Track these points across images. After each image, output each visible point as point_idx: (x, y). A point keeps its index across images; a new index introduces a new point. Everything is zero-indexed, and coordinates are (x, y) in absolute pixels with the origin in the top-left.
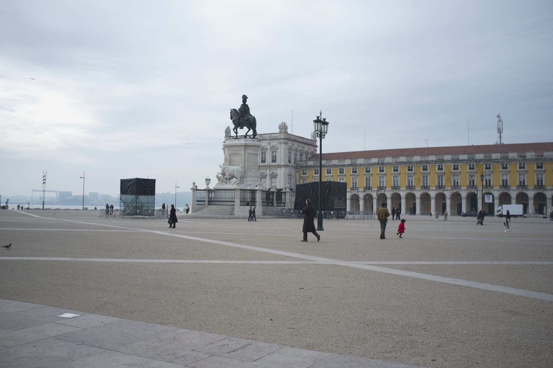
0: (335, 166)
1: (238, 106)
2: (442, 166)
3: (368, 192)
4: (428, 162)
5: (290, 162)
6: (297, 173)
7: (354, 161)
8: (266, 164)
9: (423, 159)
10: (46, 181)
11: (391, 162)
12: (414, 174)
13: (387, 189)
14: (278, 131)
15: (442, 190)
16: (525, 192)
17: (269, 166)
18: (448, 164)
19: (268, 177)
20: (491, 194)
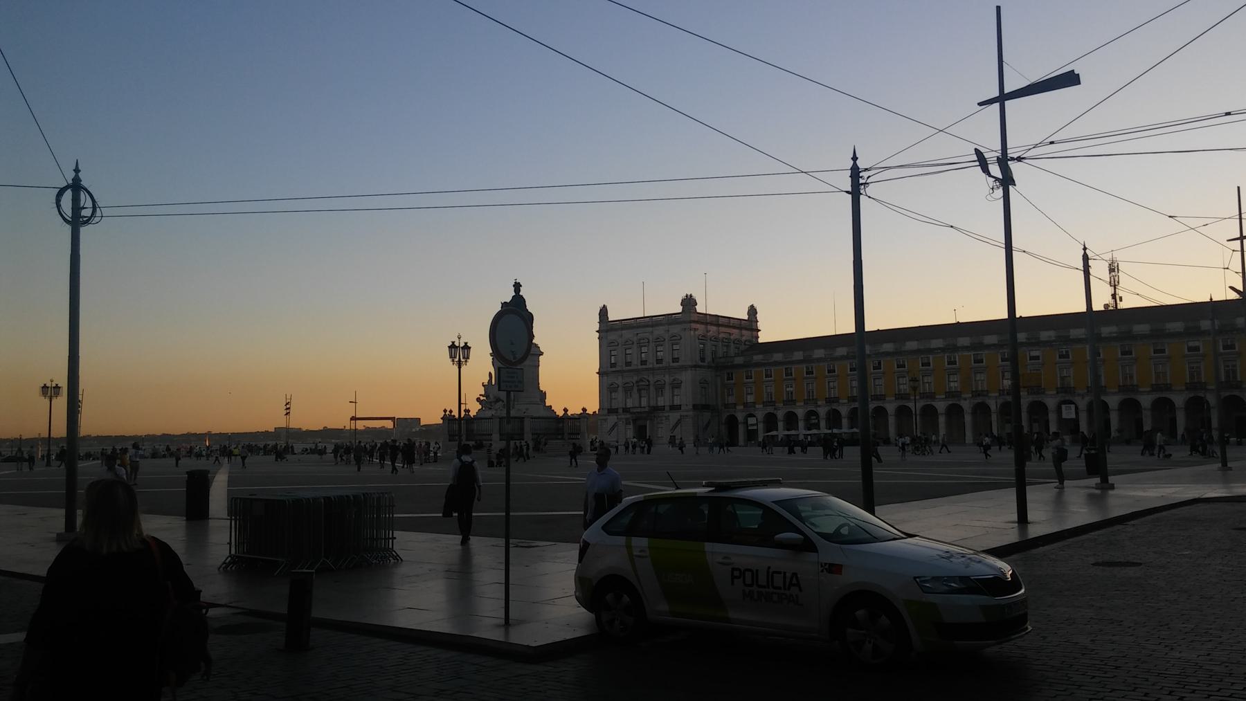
0: (777, 363)
1: (508, 296)
3: (835, 406)
4: (931, 351)
5: (703, 360)
8: (664, 364)
9: (922, 347)
10: (292, 411)
14: (679, 309)
18: (966, 353)
19: (667, 387)
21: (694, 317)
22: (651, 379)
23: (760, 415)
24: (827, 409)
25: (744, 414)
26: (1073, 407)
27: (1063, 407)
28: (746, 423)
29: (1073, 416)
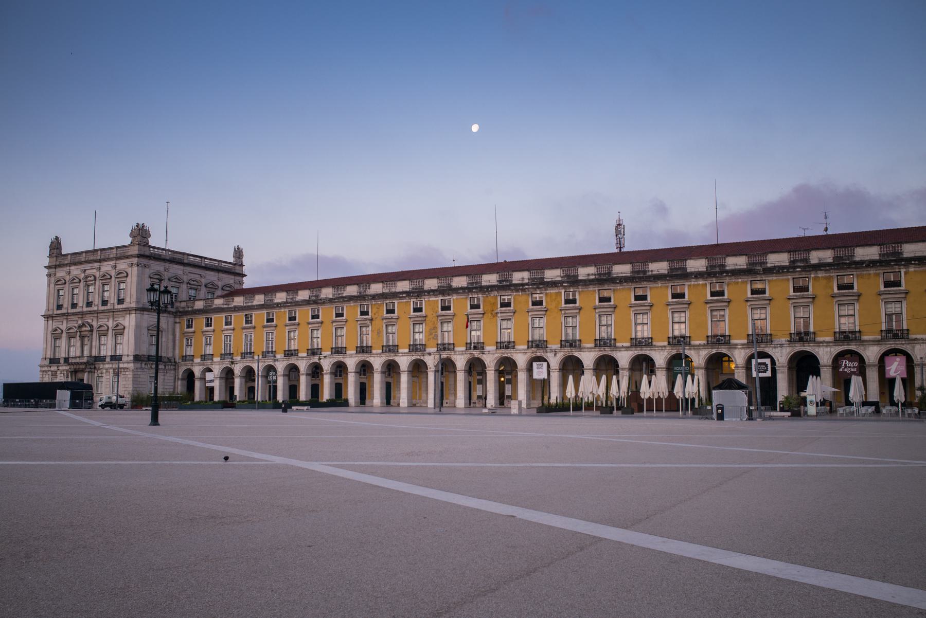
0: (237, 309)
2: (421, 304)
3: (293, 360)
4: (395, 295)
6: (177, 325)
7: (269, 297)
8: (109, 307)
9: (386, 291)
11: (331, 296)
12: (372, 320)
13: (325, 353)
14: (128, 241)
15: (420, 353)
16: (576, 354)
17: (113, 311)
18: (433, 299)
20: (546, 361)
21: (147, 252)
22: (95, 324)
23: (217, 370)
24: (285, 363)
25: (201, 368)
26: (545, 364)
27: (535, 364)
28: (203, 379)
29: (544, 375)
